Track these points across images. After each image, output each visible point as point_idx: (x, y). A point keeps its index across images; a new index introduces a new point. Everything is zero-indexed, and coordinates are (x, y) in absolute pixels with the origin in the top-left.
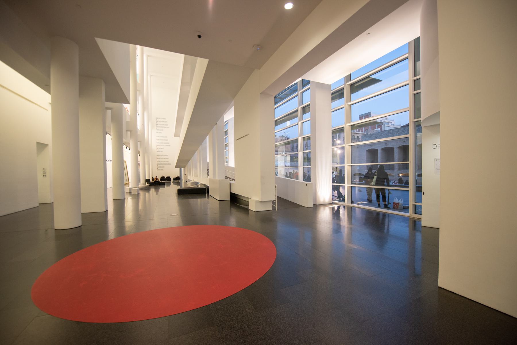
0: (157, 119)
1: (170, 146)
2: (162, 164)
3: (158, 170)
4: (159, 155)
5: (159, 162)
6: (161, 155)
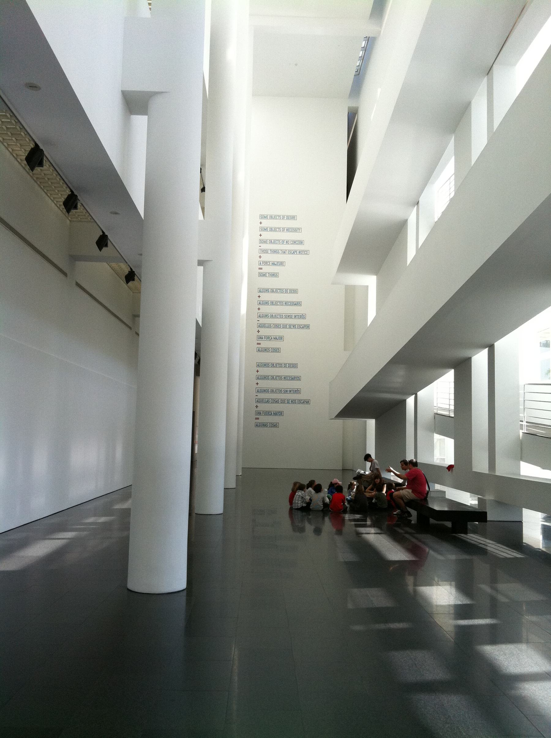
0: (264, 234)
1: (307, 327)
2: (276, 401)
4: (266, 365)
5: (265, 391)
6: (273, 365)
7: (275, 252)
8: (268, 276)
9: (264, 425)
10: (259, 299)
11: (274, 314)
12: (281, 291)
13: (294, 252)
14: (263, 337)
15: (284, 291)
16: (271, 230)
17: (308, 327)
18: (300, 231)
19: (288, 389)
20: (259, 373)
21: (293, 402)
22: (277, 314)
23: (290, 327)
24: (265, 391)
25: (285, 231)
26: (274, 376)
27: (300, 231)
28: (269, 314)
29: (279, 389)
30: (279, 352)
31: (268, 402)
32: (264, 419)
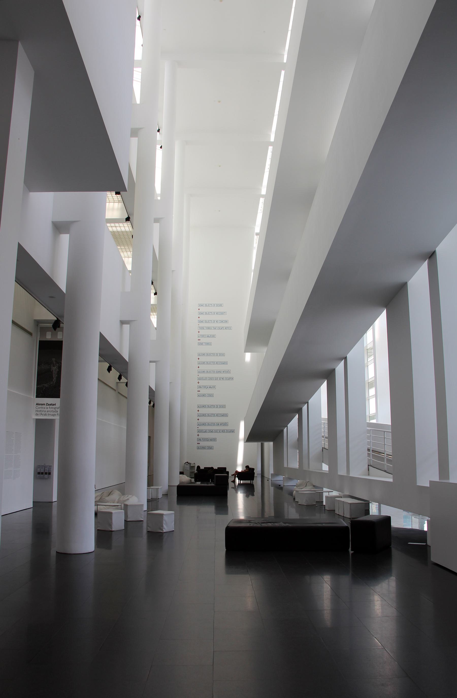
2: (211, 431)
3: (198, 448)
4: (204, 406)
5: (204, 424)
6: (209, 407)
7: (209, 328)
8: (204, 345)
9: (204, 448)
10: (199, 361)
11: (209, 371)
12: (213, 354)
13: (222, 328)
14: (202, 386)
15: (215, 354)
16: (206, 313)
17: (232, 379)
18: (226, 314)
19: (220, 423)
20: (199, 421)
21: (223, 431)
22: (211, 370)
23: (220, 379)
24: (203, 424)
25: (216, 314)
26: (210, 414)
27: (226, 314)
28: (206, 371)
29: (213, 423)
30: (213, 396)
31: (205, 432)
32: (203, 444)
